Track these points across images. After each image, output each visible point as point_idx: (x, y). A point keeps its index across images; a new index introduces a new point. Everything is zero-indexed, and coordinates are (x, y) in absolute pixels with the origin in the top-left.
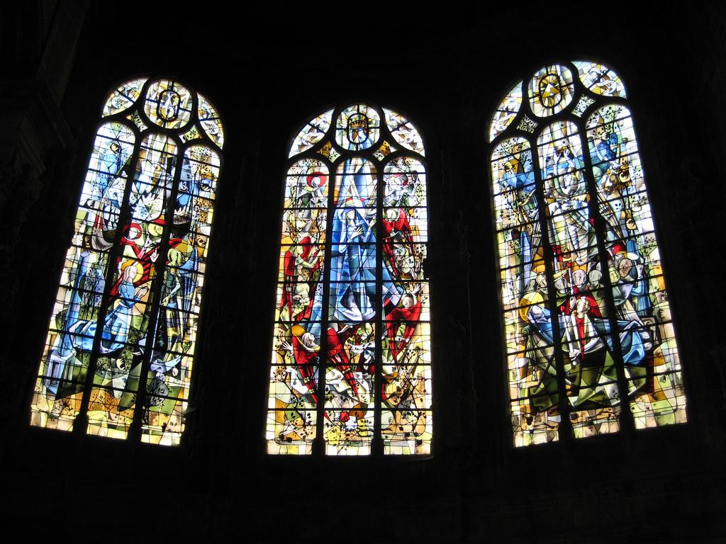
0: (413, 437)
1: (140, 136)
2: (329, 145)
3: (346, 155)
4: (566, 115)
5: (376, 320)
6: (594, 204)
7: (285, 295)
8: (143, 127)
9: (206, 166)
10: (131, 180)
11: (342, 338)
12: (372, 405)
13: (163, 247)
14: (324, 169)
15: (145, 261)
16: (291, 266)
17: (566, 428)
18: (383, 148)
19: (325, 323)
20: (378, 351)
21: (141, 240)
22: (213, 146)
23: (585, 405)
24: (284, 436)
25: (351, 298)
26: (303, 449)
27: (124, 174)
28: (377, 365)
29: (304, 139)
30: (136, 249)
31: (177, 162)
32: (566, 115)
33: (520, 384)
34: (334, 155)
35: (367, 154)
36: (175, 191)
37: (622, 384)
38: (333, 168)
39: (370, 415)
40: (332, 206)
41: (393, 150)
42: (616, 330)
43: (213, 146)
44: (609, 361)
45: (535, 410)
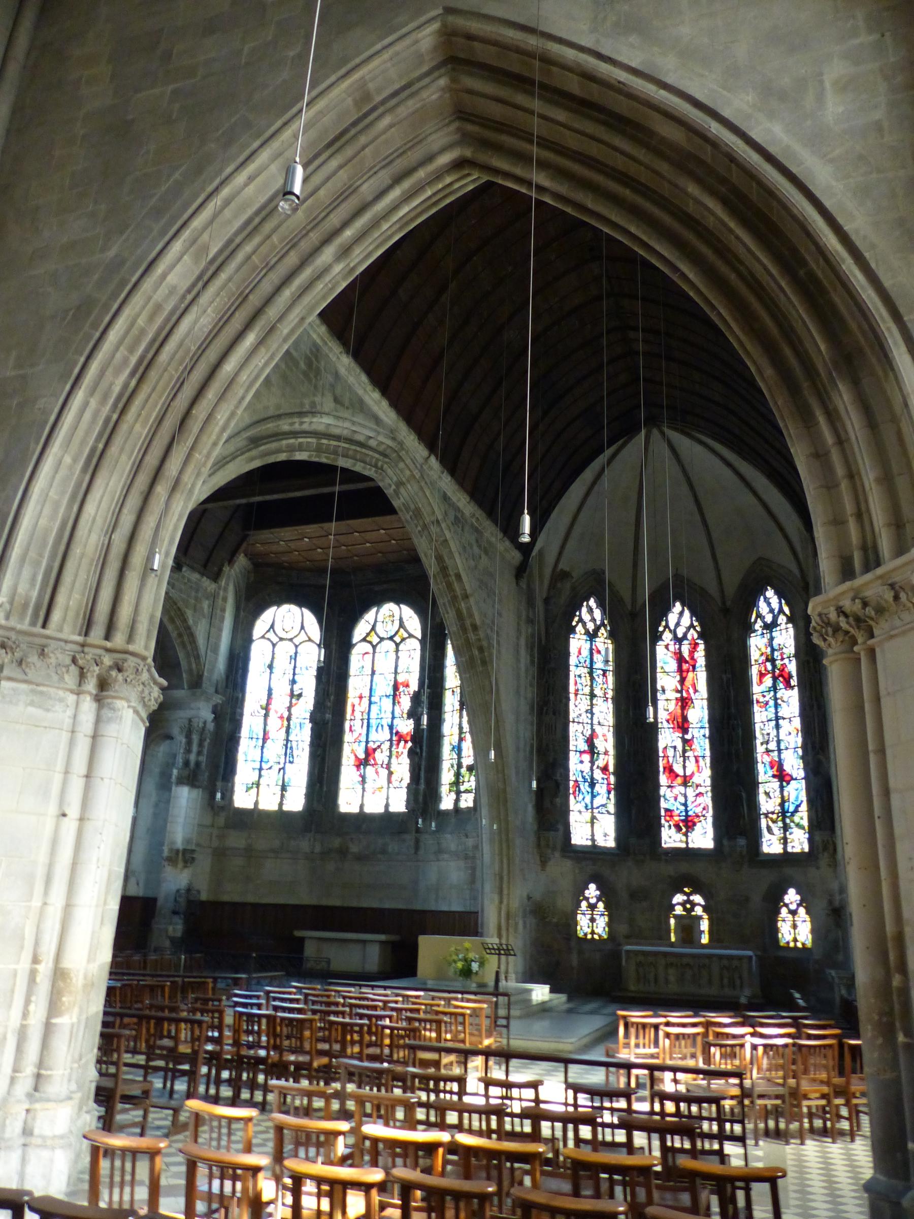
1: (274, 645)
2: (373, 633)
3: (382, 639)
5: (391, 740)
7: (351, 727)
8: (275, 639)
9: (312, 656)
10: (271, 672)
12: (385, 785)
13: (289, 709)
14: (370, 649)
15: (281, 717)
16: (353, 711)
17: (457, 801)
18: (400, 633)
19: (367, 742)
20: (390, 757)
21: (280, 703)
22: (312, 641)
23: (467, 791)
24: (349, 800)
25: (380, 727)
26: (355, 810)
27: (268, 671)
28: (388, 767)
29: (361, 629)
30: (276, 712)
31: (295, 657)
33: (447, 776)
34: (375, 640)
35: (391, 638)
36: (294, 674)
38: (374, 647)
39: (385, 790)
40: (373, 672)
41: (406, 635)
43: (312, 641)
45: (450, 791)
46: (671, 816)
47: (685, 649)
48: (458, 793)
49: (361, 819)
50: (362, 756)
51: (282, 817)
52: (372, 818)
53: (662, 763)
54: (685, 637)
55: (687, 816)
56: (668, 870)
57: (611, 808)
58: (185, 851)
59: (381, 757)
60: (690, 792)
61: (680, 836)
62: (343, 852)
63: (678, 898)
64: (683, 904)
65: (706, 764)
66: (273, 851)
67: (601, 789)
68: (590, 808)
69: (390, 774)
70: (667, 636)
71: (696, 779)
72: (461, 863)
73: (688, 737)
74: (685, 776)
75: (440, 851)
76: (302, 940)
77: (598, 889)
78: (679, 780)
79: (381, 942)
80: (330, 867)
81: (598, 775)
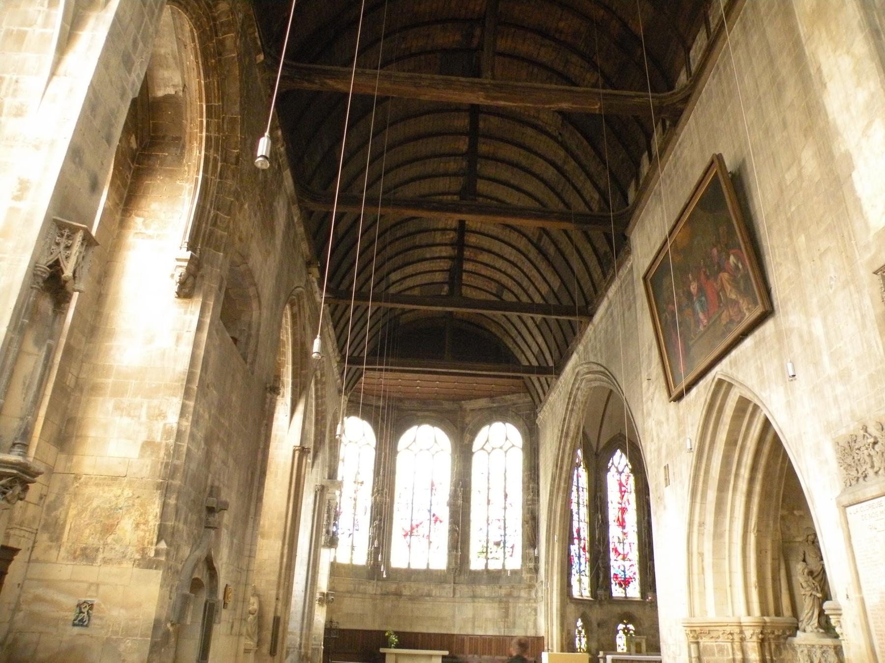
0: (440, 561)
4: (501, 448)
6: (505, 488)
11: (417, 526)
28: (429, 536)
32: (501, 448)
37: (505, 553)
42: (505, 535)
44: (502, 545)
46: (617, 578)
47: (623, 478)
48: (487, 559)
49: (410, 574)
50: (408, 529)
51: (352, 570)
52: (417, 572)
53: (611, 546)
54: (623, 472)
55: (625, 578)
56: (618, 609)
57: (588, 573)
58: (328, 594)
59: (423, 530)
60: (627, 564)
61: (621, 590)
62: (398, 594)
63: (621, 626)
64: (623, 630)
65: (635, 547)
66: (348, 592)
67: (583, 560)
68: (580, 572)
69: (430, 542)
70: (613, 470)
71: (629, 557)
72: (496, 605)
73: (625, 531)
74: (624, 555)
75: (474, 597)
76: (384, 654)
77: (582, 621)
78: (621, 556)
79: (444, 657)
80: (388, 605)
81: (582, 552)
